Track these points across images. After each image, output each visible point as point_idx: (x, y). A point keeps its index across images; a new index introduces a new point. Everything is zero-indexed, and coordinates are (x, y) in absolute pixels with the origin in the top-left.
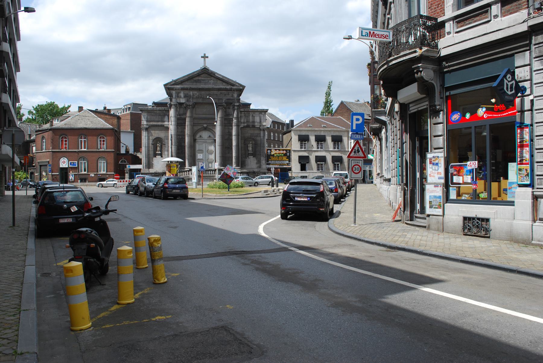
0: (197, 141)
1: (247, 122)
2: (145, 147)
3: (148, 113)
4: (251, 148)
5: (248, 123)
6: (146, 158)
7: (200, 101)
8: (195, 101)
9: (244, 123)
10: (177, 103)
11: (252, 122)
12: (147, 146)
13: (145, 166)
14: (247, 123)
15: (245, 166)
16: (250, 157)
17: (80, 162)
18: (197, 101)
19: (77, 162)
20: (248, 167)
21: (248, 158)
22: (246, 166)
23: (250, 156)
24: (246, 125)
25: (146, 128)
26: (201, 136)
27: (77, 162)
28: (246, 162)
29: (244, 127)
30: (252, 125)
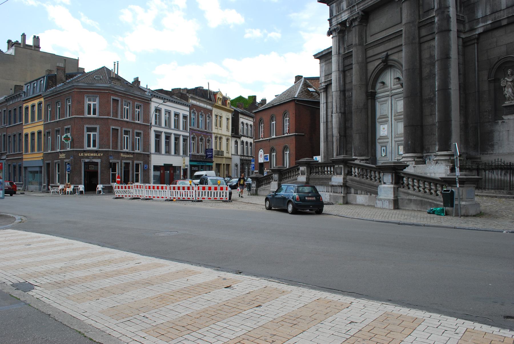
0: (377, 96)
1: (492, 13)
2: (324, 122)
3: (326, 61)
4: (510, 90)
5: (497, 15)
6: (324, 143)
7: (369, 3)
8: (362, 7)
9: (485, 18)
10: (337, 24)
11: (507, 8)
12: (325, 121)
13: (324, 156)
14: (493, 16)
15: (492, 146)
16: (505, 117)
17: (285, 152)
18: (364, 6)
19: (268, 155)
20: (501, 152)
21: (500, 122)
22: (496, 147)
23: (506, 115)
24: (490, 22)
25: (324, 88)
26: (383, 83)
27: (268, 155)
28: (496, 134)
29: (485, 32)
30: (508, 18)
